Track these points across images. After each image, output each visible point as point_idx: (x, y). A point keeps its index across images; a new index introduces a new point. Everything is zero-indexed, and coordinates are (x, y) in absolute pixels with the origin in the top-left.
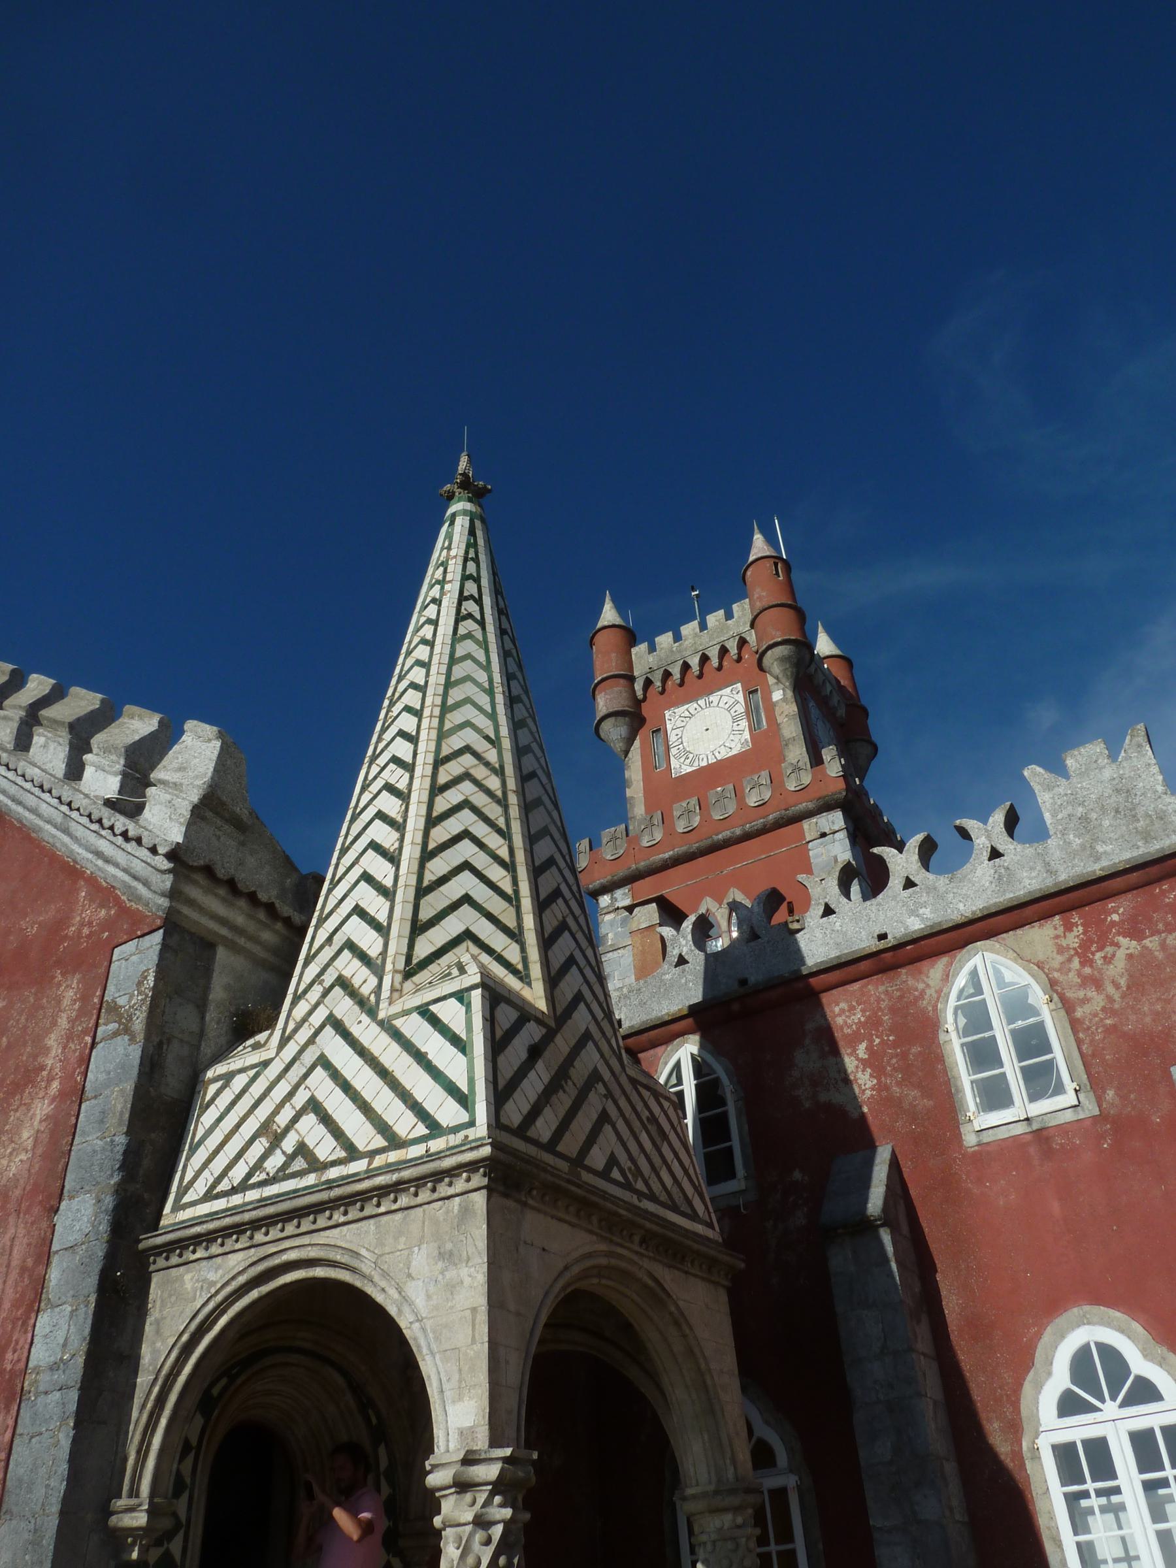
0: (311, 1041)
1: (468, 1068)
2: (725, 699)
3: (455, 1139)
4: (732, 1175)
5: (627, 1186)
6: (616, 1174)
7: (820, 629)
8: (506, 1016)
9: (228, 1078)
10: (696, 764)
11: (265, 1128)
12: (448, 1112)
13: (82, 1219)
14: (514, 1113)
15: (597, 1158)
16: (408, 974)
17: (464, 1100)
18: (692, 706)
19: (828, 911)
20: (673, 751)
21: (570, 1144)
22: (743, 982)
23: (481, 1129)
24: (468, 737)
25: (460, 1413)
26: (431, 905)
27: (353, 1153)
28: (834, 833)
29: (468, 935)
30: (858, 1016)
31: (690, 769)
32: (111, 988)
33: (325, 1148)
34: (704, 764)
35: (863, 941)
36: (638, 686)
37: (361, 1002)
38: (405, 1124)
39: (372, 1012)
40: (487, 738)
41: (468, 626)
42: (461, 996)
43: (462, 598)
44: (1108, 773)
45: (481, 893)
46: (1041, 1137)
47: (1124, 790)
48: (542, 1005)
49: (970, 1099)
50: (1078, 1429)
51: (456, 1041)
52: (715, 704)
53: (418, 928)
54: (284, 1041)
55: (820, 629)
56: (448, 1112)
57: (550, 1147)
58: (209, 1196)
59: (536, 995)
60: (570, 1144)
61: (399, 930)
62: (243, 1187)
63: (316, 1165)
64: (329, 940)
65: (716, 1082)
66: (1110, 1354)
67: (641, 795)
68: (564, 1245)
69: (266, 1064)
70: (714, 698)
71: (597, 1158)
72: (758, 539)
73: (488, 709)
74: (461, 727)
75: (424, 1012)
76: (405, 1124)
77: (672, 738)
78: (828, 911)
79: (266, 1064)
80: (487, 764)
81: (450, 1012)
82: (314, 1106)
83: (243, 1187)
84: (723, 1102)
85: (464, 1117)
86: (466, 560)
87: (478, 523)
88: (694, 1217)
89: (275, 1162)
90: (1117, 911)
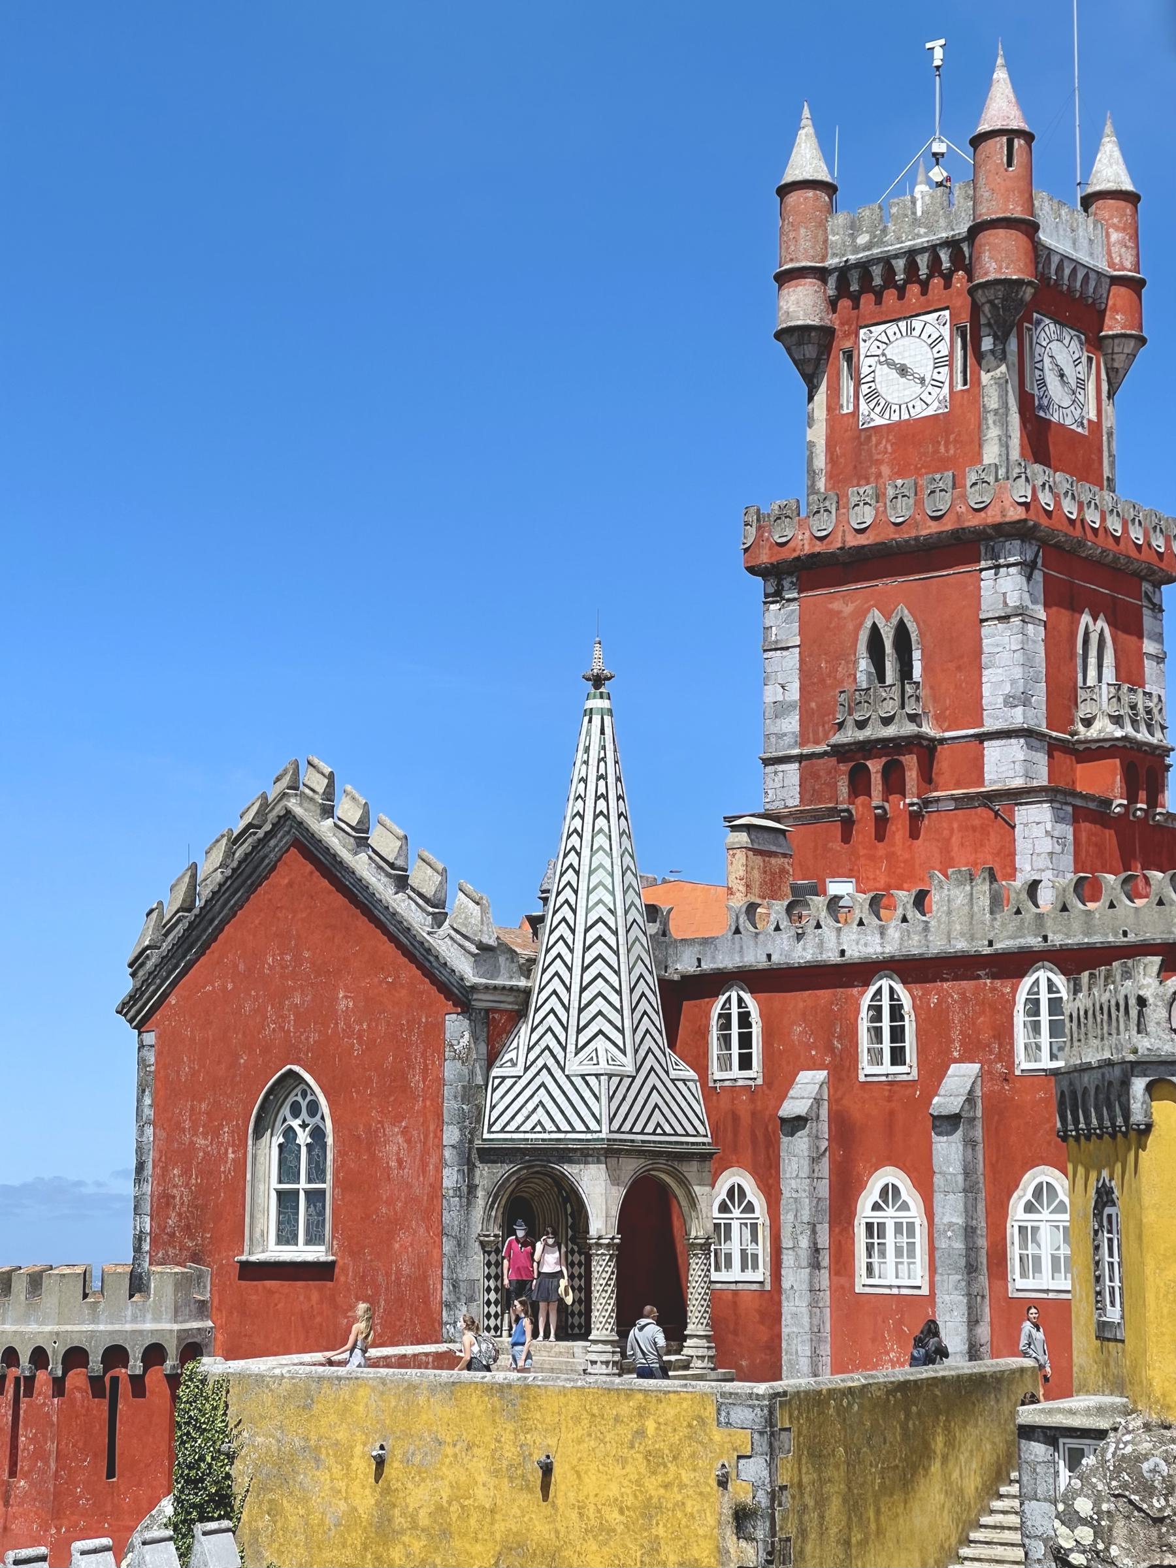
0: (538, 1074)
2: (929, 329)
3: (595, 1136)
4: (750, 1068)
5: (665, 1134)
6: (659, 1131)
7: (1108, 129)
8: (615, 1080)
9: (504, 1078)
10: (887, 416)
12: (593, 1125)
14: (616, 1125)
15: (650, 1129)
16: (576, 1054)
17: (598, 1122)
18: (892, 328)
19: (818, 926)
20: (864, 389)
21: (637, 1129)
24: (601, 911)
26: (586, 1016)
27: (559, 1131)
28: (1008, 566)
29: (600, 1032)
31: (879, 422)
32: (448, 1035)
33: (549, 1126)
34: (895, 417)
35: (831, 956)
36: (832, 281)
37: (558, 1062)
38: (579, 1126)
39: (563, 1069)
40: (610, 910)
41: (601, 821)
42: (597, 1076)
43: (597, 798)
45: (607, 1010)
46: (893, 1084)
48: (630, 1069)
49: (864, 1057)
50: (876, 1217)
51: (595, 1095)
52: (916, 333)
53: (579, 1031)
54: (526, 1069)
55: (1108, 129)
56: (593, 1125)
57: (630, 1132)
58: (502, 1131)
59: (628, 1064)
60: (637, 1129)
61: (572, 1030)
62: (517, 1131)
63: (545, 1131)
64: (541, 1022)
65: (748, 1014)
66: (895, 1188)
67: (823, 442)
69: (520, 1077)
70: (917, 323)
71: (650, 1129)
72: (1001, 75)
73: (610, 888)
74: (597, 904)
75: (583, 1076)
77: (865, 370)
79: (520, 1077)
80: (610, 928)
81: (592, 1081)
83: (517, 1131)
84: (750, 1026)
85: (598, 1129)
86: (599, 761)
87: (607, 719)
88: (698, 1134)
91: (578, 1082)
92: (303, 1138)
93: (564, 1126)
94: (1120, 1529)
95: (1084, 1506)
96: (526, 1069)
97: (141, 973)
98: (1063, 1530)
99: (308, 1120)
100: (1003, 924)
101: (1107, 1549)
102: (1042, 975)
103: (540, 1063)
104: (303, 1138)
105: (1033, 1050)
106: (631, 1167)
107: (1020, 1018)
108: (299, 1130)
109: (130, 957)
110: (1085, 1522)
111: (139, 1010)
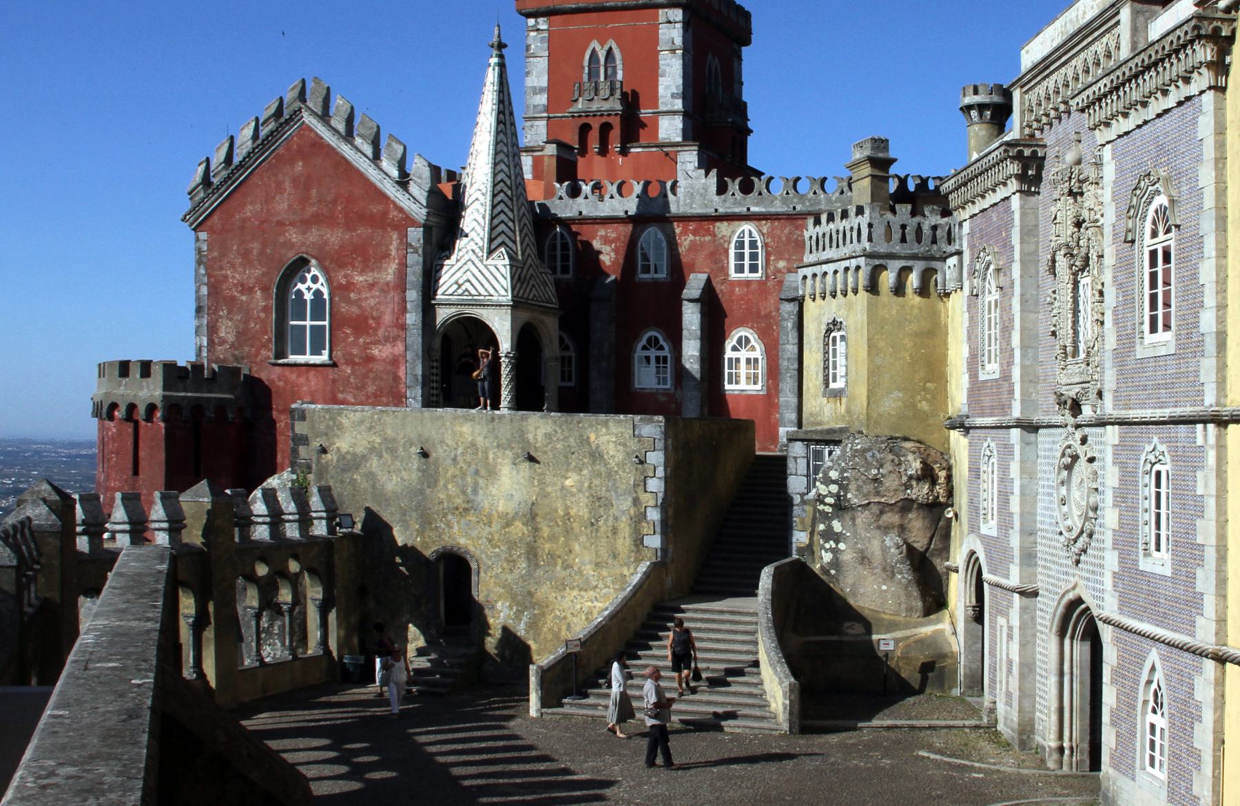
1: (507, 283)
11: (456, 283)
13: (413, 295)
19: (612, 197)
22: (580, 213)
23: (510, 297)
25: (505, 345)
30: (614, 235)
33: (473, 292)
38: (492, 291)
39: (481, 261)
44: (703, 181)
47: (706, 190)
54: (458, 261)
68: (525, 316)
76: (492, 291)
78: (612, 197)
81: (503, 270)
82: (468, 281)
89: (460, 291)
90: (692, 226)
91: (492, 269)
92: (308, 296)
93: (483, 292)
94: (852, 487)
95: (834, 475)
96: (458, 261)
97: (197, 199)
98: (823, 487)
99: (312, 285)
100: (725, 201)
101: (845, 495)
102: (747, 227)
103: (467, 258)
104: (308, 296)
105: (740, 269)
106: (525, 316)
107: (732, 252)
108: (305, 292)
109: (189, 189)
110: (834, 482)
111: (199, 221)
